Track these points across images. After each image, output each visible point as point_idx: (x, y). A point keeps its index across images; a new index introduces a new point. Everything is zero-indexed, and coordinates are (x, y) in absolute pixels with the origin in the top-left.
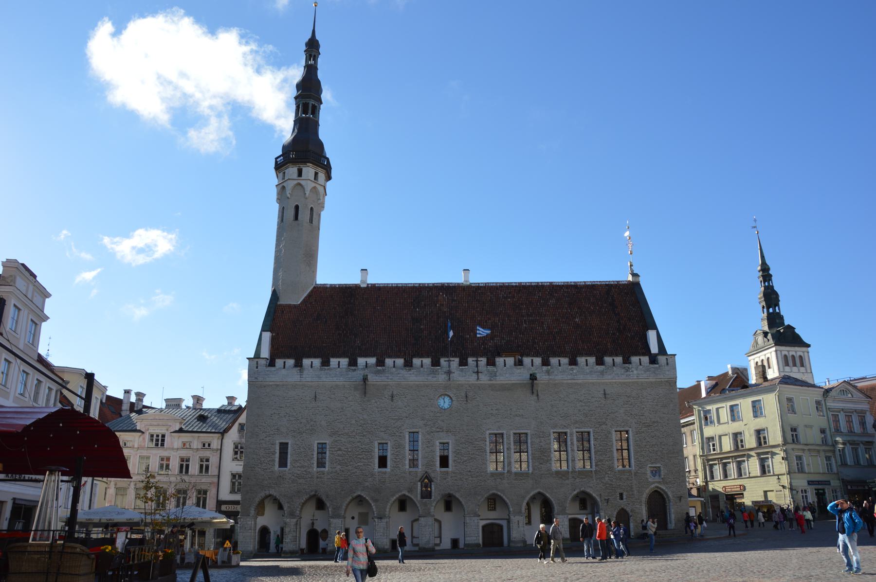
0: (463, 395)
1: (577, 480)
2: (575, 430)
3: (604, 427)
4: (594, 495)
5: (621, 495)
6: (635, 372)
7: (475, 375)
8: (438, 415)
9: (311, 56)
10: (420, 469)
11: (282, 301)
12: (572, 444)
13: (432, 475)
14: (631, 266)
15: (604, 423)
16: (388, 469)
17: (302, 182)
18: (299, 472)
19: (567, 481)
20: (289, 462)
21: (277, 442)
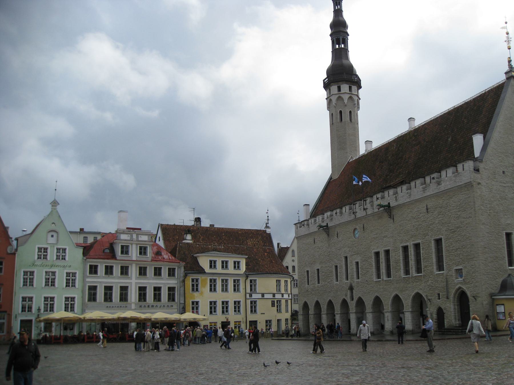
0: (362, 226)
2: (412, 243)
3: (427, 237)
5: (439, 294)
6: (443, 185)
9: (336, 3)
13: (353, 285)
14: (510, 61)
17: (331, 98)
19: (409, 285)
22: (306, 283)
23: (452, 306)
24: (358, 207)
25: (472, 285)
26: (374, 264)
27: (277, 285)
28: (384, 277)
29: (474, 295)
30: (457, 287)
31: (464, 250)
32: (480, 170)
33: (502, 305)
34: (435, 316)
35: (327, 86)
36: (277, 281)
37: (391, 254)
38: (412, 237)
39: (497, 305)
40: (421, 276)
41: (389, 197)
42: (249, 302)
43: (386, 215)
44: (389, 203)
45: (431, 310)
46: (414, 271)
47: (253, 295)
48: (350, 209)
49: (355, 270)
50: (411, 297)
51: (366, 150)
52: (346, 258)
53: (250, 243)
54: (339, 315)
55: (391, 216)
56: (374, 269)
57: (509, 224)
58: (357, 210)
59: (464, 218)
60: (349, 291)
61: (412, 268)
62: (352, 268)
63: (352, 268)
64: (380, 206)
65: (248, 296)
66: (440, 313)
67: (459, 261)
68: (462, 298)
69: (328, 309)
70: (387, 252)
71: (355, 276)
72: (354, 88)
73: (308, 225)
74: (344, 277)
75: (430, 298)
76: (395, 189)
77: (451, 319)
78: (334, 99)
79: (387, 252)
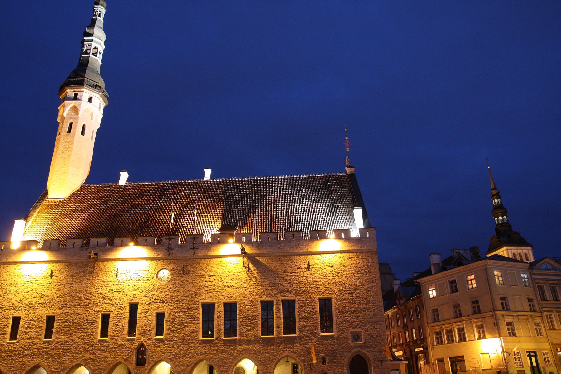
1: (282, 346)
7: (191, 250)
12: (278, 311)
20: (18, 335)
21: (11, 316)
25: (376, 349)
30: (354, 351)
31: (365, 313)
33: (397, 370)
49: (154, 322)
67: (358, 324)
71: (154, 332)
74: (126, 331)
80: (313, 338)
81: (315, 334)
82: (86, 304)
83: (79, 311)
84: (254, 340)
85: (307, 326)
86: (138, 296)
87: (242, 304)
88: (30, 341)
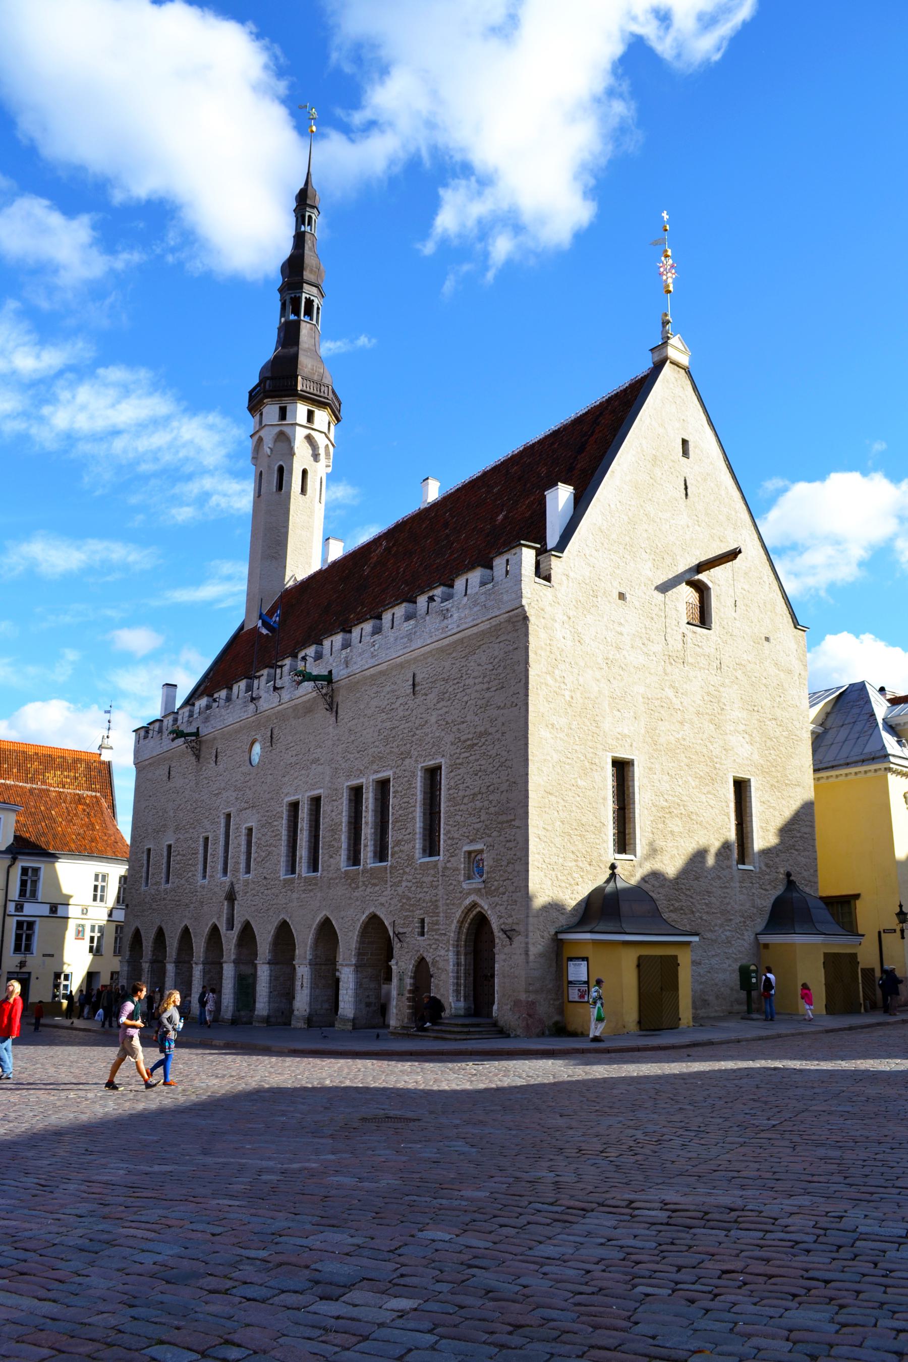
1: (369, 890)
3: (407, 761)
4: (386, 923)
6: (456, 616)
8: (247, 779)
10: (227, 879)
11: (245, 630)
13: (236, 889)
15: (408, 755)
16: (206, 882)
18: (153, 892)
22: (143, 881)
23: (451, 956)
24: (262, 684)
25: (505, 898)
26: (284, 833)
27: (96, 887)
28: (303, 867)
29: (507, 928)
30: (467, 902)
32: (553, 578)
34: (408, 981)
35: (255, 403)
36: (97, 876)
37: (324, 808)
38: (373, 762)
39: (571, 959)
40: (386, 868)
41: (332, 654)
42: (12, 923)
43: (322, 705)
44: (330, 672)
45: (402, 965)
46: (370, 854)
47: (26, 905)
48: (249, 688)
49: (243, 848)
50: (358, 926)
51: (324, 560)
52: (228, 816)
53: (53, 781)
54: (200, 967)
55: (332, 706)
56: (283, 849)
57: (624, 736)
58: (262, 693)
59: (499, 707)
60: (226, 903)
61: (366, 846)
62: (238, 842)
63: (238, 842)
64: (307, 677)
65: (11, 907)
66: (422, 972)
68: (478, 937)
69: (180, 950)
70: (316, 801)
71: (242, 866)
72: (322, 417)
73: (160, 731)
74: (220, 867)
75: (401, 930)
76: (348, 635)
77: (448, 989)
78: (268, 435)
79: (316, 801)
80: (407, 870)
81: (411, 858)
82: (191, 821)
83: (187, 835)
84: (336, 878)
85: (402, 840)
86: (231, 798)
87: (326, 797)
88: (156, 887)
